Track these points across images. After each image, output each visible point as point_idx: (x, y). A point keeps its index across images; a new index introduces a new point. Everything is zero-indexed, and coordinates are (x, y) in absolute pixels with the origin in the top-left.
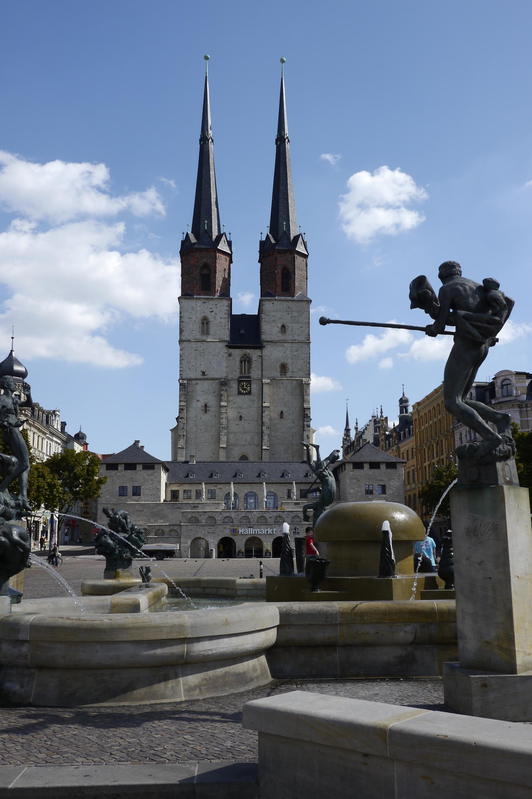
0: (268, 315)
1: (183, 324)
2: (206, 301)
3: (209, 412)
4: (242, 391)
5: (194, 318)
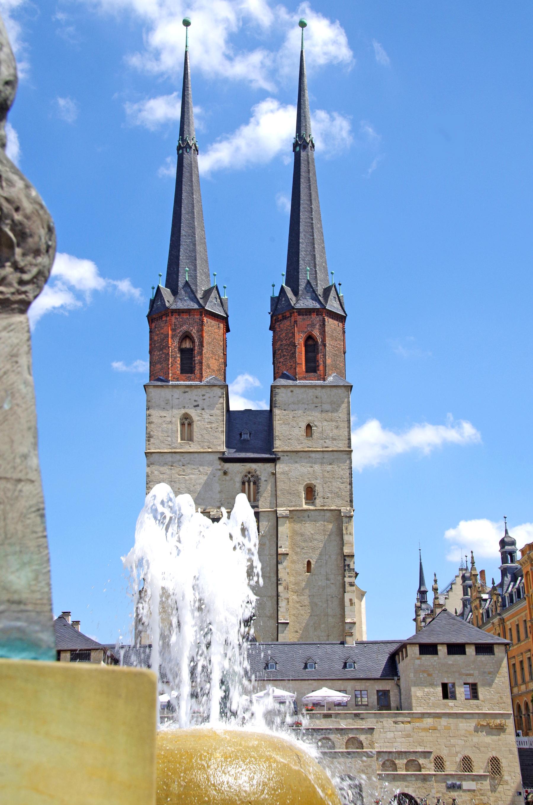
1: (152, 425)
2: (187, 390)
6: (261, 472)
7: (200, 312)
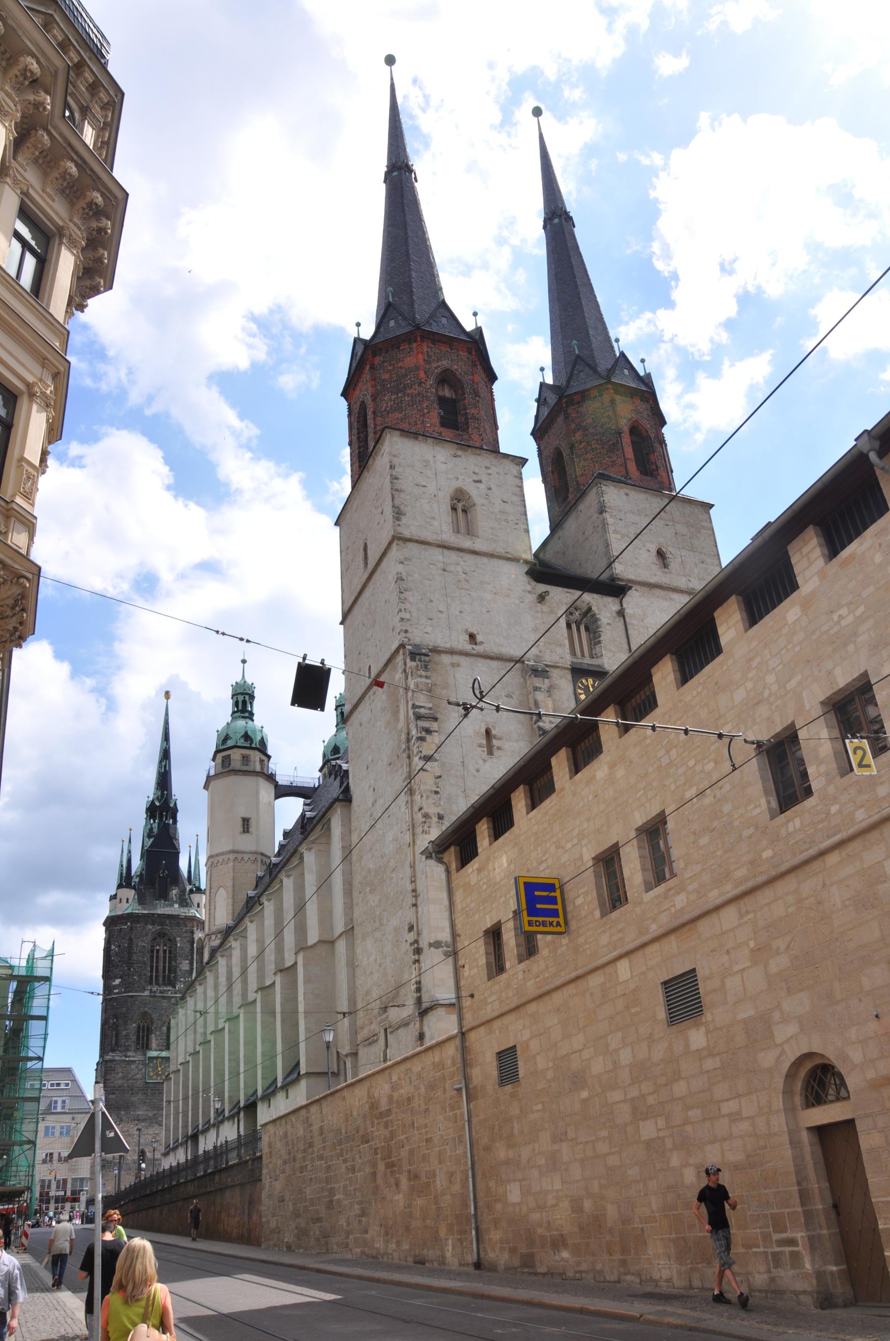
0: (621, 519)
6: (599, 609)
7: (468, 348)
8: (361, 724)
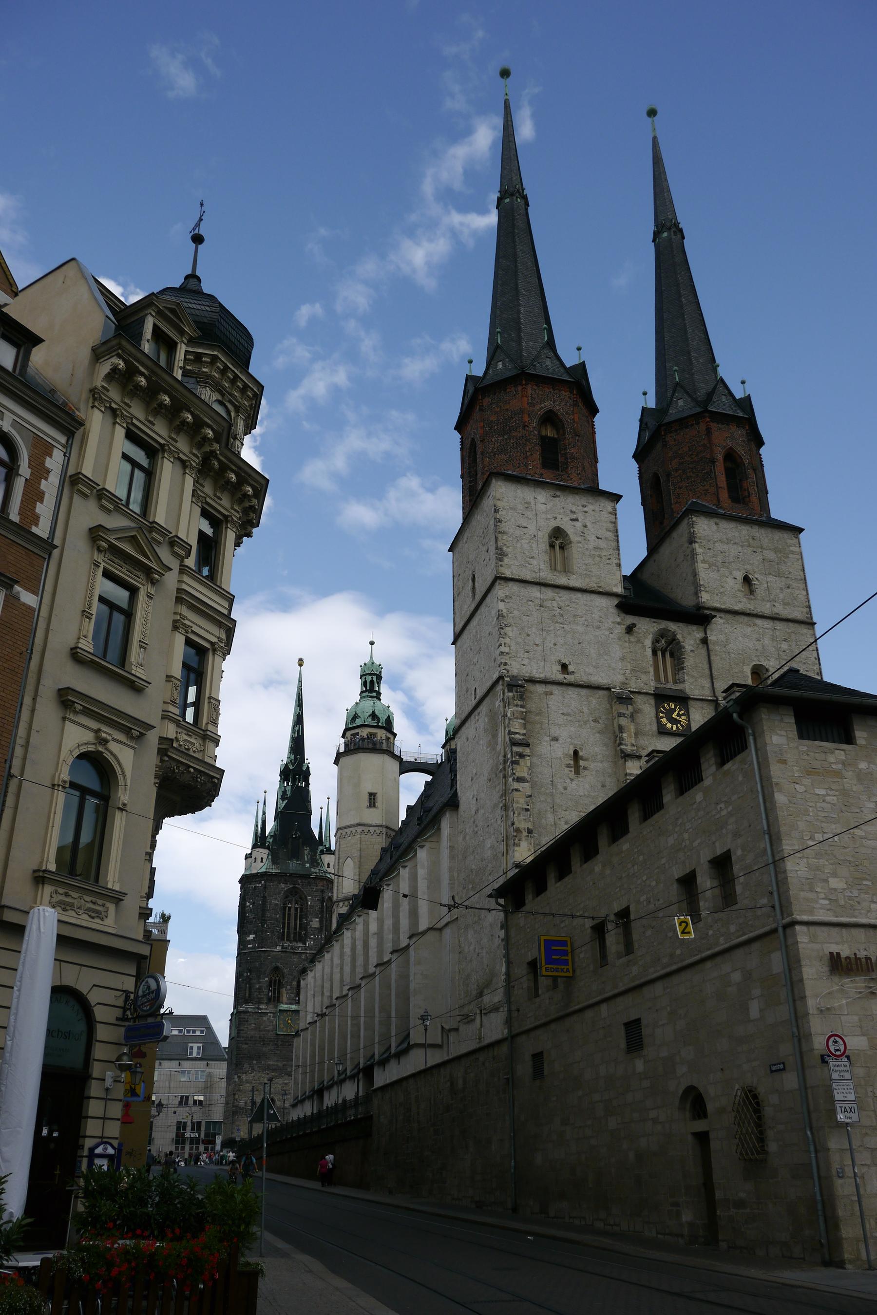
0: (710, 549)
3: (586, 772)
4: (669, 725)
5: (532, 529)
8: (468, 739)
